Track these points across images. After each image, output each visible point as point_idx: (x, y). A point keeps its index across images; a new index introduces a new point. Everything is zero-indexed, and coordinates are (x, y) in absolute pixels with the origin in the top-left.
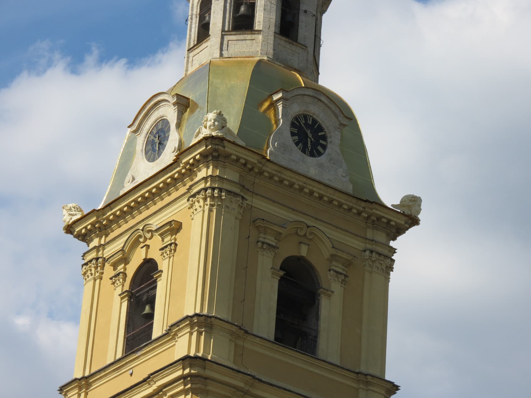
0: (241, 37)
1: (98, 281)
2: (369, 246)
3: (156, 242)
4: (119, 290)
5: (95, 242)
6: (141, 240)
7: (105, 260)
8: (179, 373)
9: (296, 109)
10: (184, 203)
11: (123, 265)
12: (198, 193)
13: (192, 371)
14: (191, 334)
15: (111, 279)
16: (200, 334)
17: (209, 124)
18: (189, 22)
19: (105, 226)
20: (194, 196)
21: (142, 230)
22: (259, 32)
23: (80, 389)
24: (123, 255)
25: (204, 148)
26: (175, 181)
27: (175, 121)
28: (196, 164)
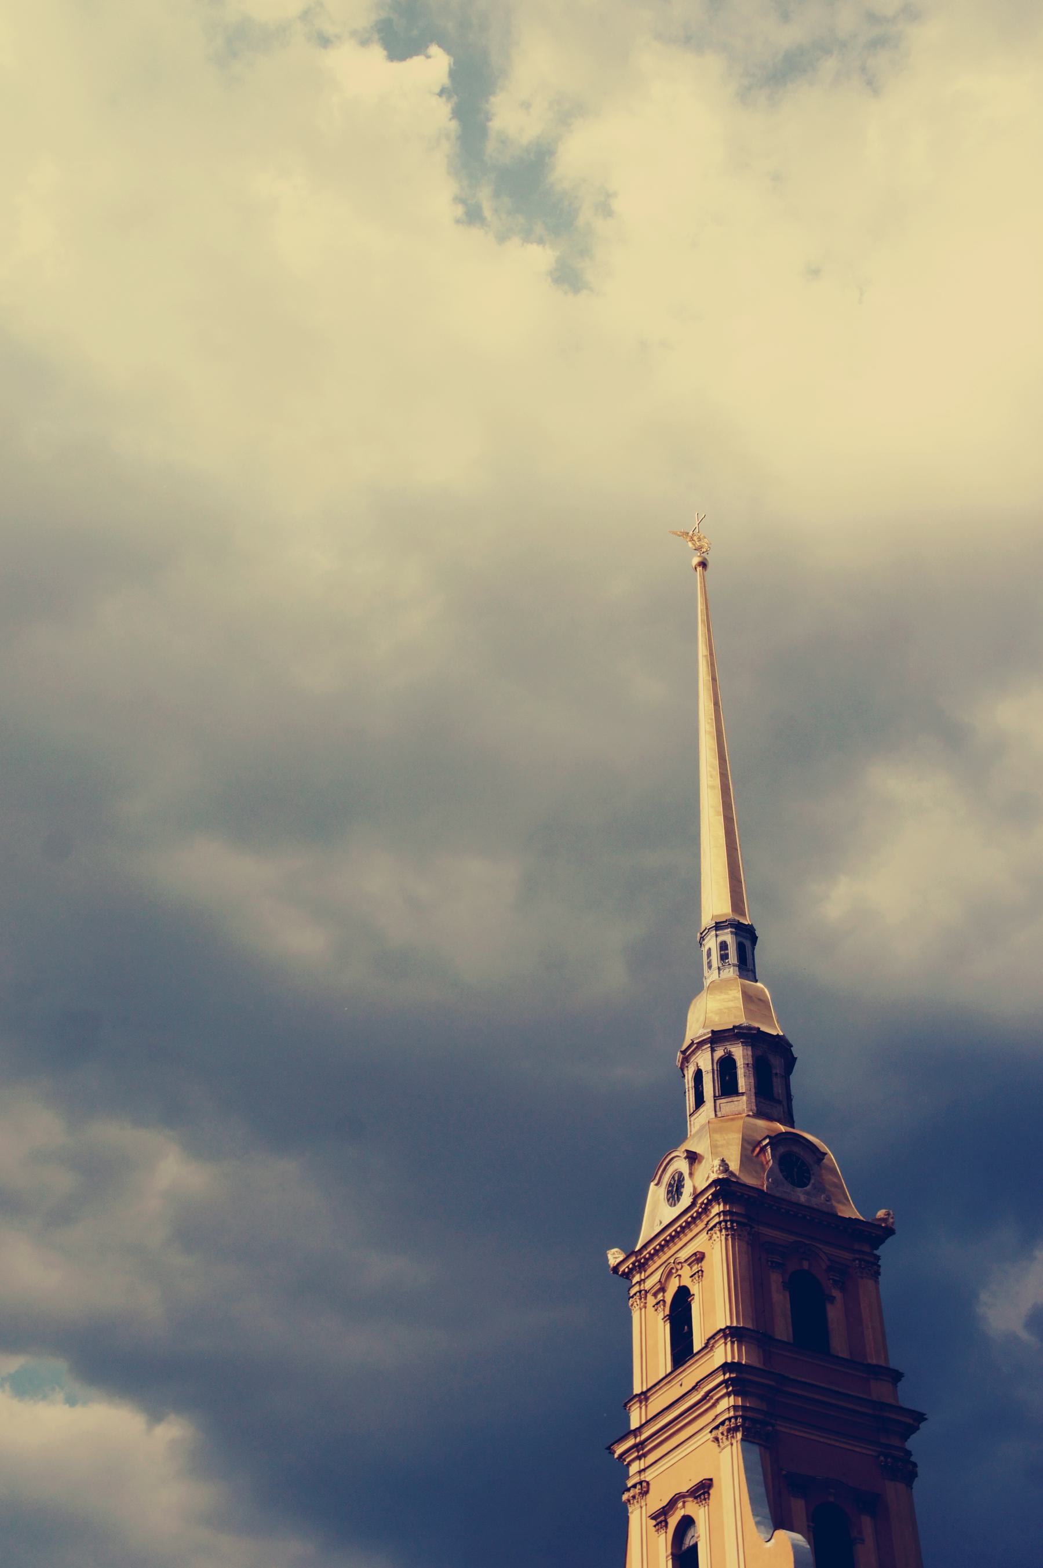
0: (730, 1099)
1: (643, 1310)
2: (857, 1256)
3: (686, 1271)
4: (661, 1315)
5: (637, 1278)
6: (674, 1271)
7: (646, 1292)
8: (721, 1378)
9: (782, 1150)
10: (704, 1236)
11: (662, 1294)
12: (715, 1226)
13: (732, 1376)
14: (726, 1344)
15: (654, 1306)
16: (733, 1343)
17: (715, 1169)
18: (687, 1094)
19: (643, 1263)
20: (711, 1229)
21: (674, 1263)
22: (743, 1094)
23: (641, 1403)
24: (661, 1285)
25: (714, 1189)
26: (694, 1219)
27: (688, 1172)
28: (709, 1202)
